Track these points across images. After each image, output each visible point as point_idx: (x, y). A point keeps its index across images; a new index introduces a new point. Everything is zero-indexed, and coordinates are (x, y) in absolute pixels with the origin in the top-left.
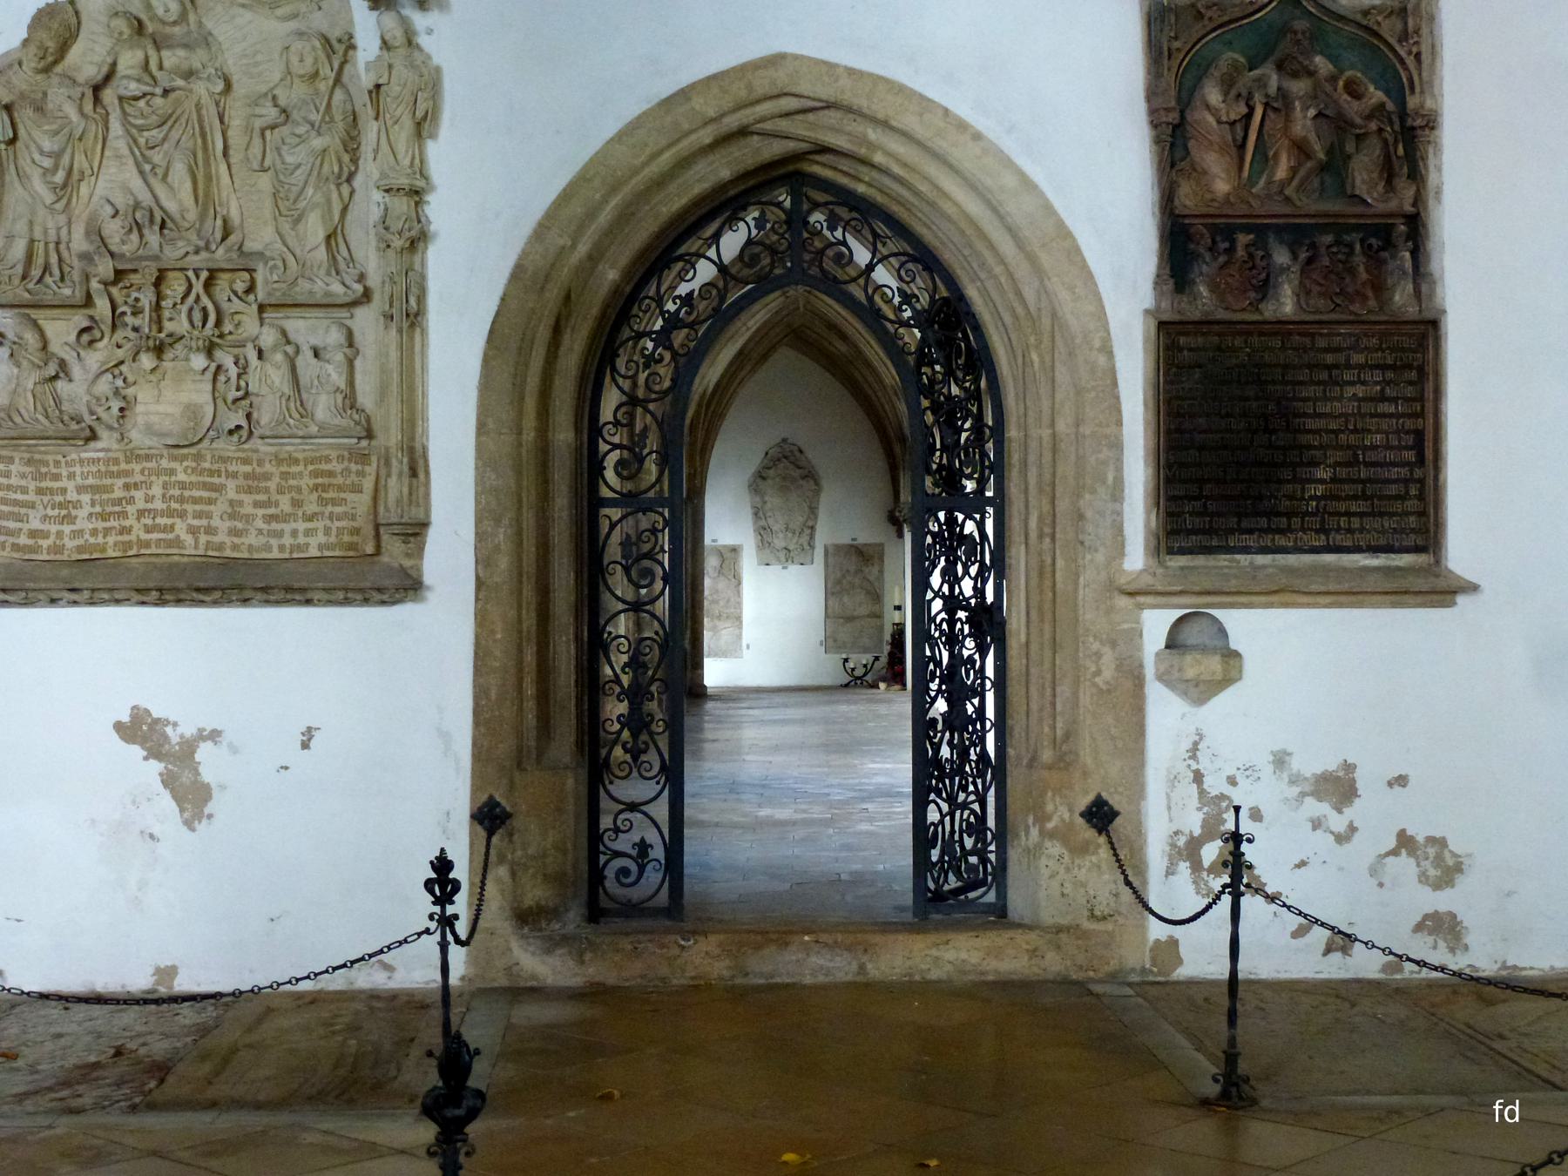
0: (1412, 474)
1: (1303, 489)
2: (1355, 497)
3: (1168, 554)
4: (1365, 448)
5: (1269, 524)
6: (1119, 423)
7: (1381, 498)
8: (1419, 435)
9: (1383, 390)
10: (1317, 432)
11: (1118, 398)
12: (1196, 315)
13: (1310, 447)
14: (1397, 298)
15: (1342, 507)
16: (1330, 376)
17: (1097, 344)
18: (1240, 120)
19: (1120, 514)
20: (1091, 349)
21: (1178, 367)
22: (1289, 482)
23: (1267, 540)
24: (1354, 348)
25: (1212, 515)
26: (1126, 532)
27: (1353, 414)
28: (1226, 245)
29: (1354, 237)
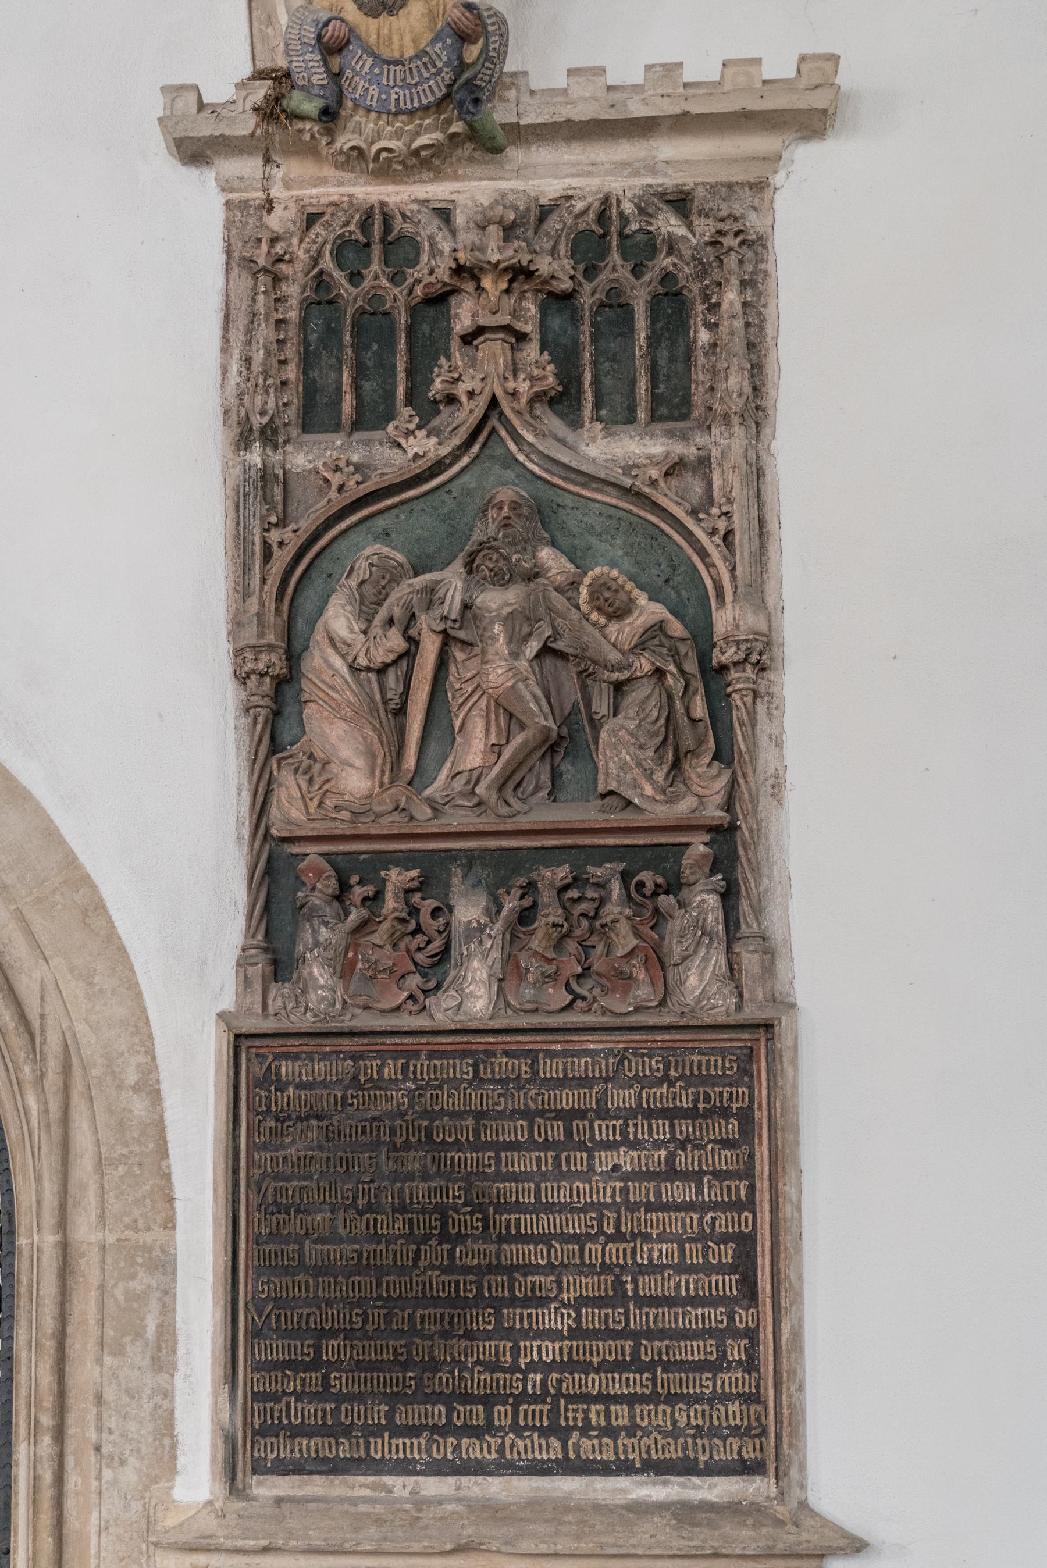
0: (731, 1319)
1: (516, 1351)
2: (619, 1366)
3: (254, 1472)
4: (641, 1270)
5: (449, 1417)
6: (169, 1224)
7: (668, 1367)
8: (746, 1243)
9: (671, 1159)
10: (544, 1239)
11: (167, 1177)
12: (306, 1022)
13: (529, 1269)
14: (692, 980)
15: (594, 1383)
16: (569, 1133)
17: (132, 1077)
18: (395, 662)
19: (168, 1394)
20: (119, 1087)
21: (277, 1120)
22: (488, 1336)
23: (446, 1448)
24: (613, 1078)
25: (340, 1399)
26: (180, 1428)
27: (614, 1206)
28: (370, 890)
29: (606, 870)
